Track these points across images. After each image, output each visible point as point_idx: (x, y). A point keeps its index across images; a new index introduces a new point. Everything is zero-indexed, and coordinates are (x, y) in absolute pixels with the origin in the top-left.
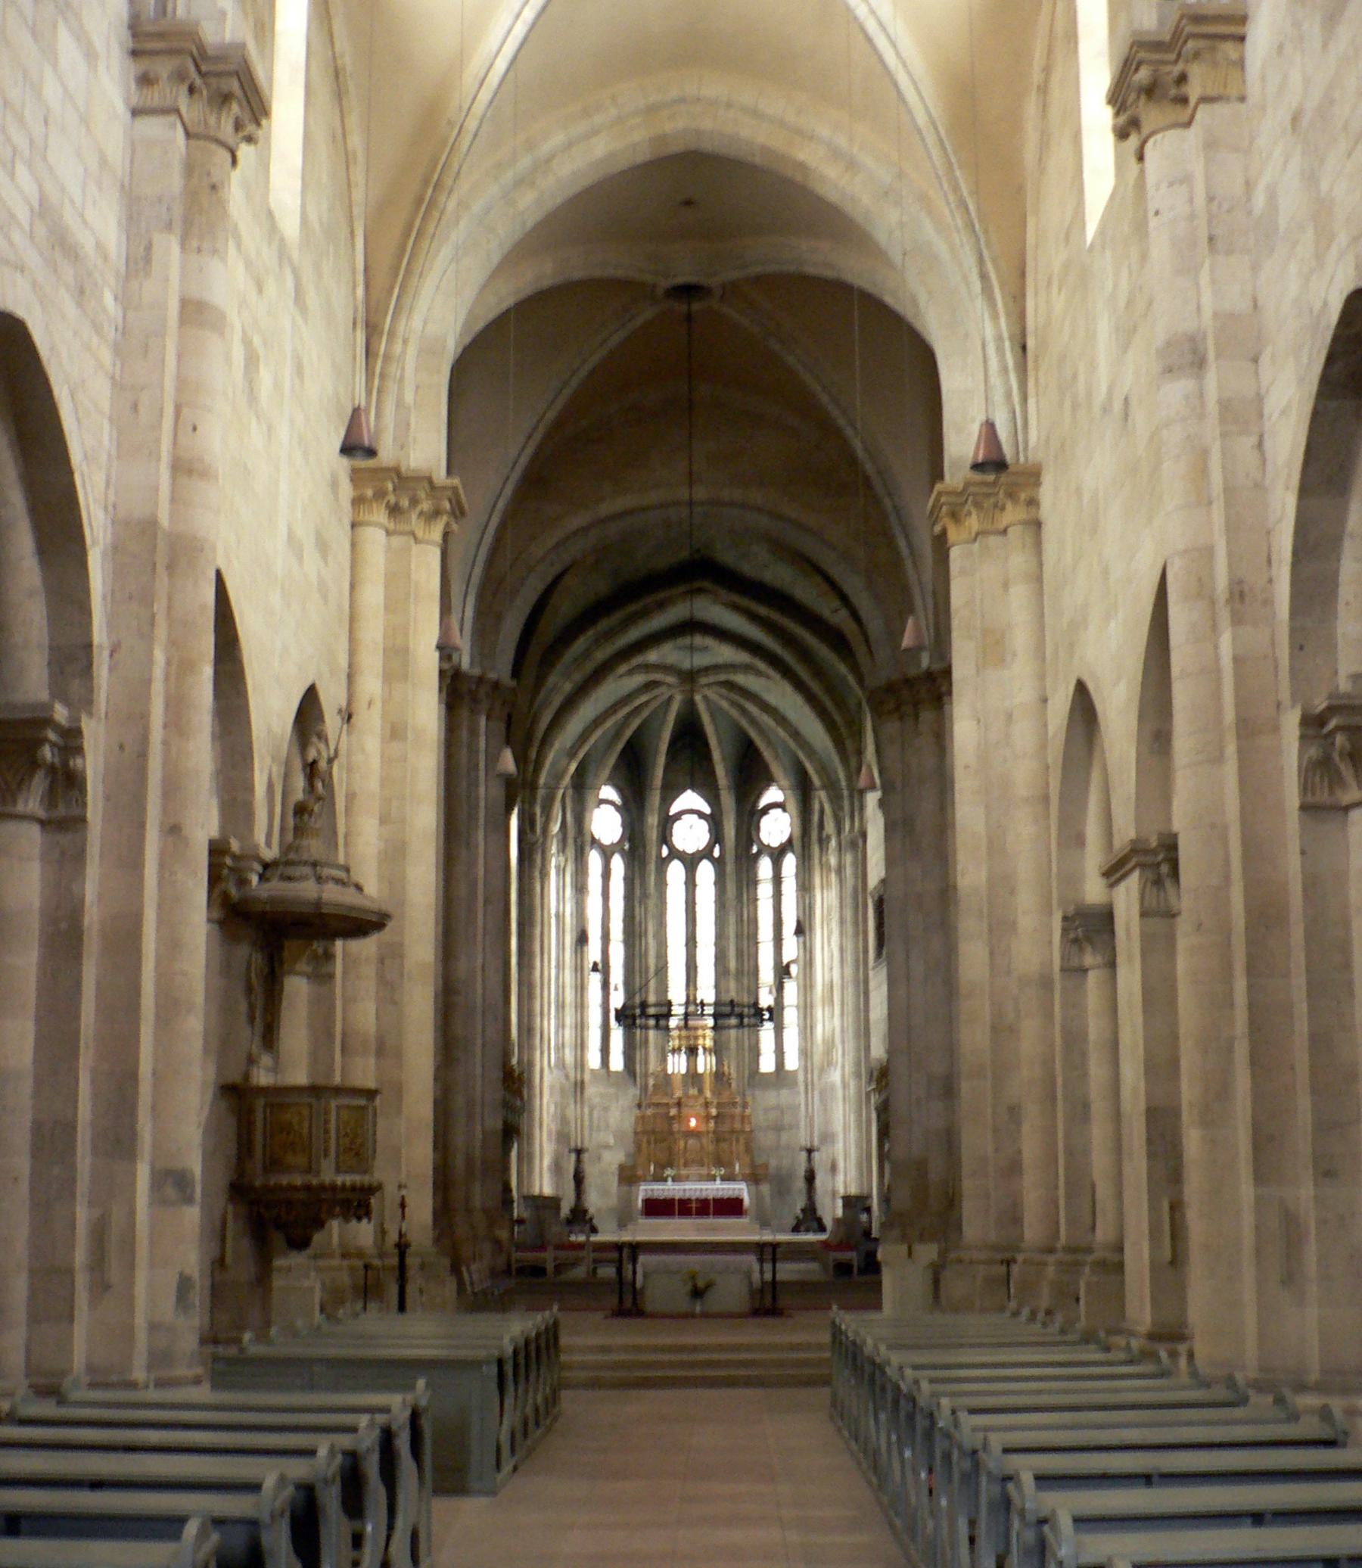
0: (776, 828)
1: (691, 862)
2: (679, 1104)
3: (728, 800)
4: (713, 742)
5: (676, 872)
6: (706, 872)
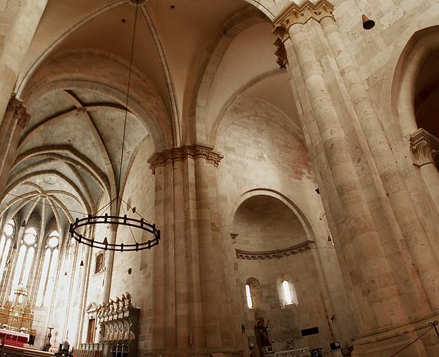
0: (53, 242)
1: (28, 247)
2: (13, 308)
3: (43, 232)
4: (43, 219)
5: (23, 248)
6: (32, 250)
